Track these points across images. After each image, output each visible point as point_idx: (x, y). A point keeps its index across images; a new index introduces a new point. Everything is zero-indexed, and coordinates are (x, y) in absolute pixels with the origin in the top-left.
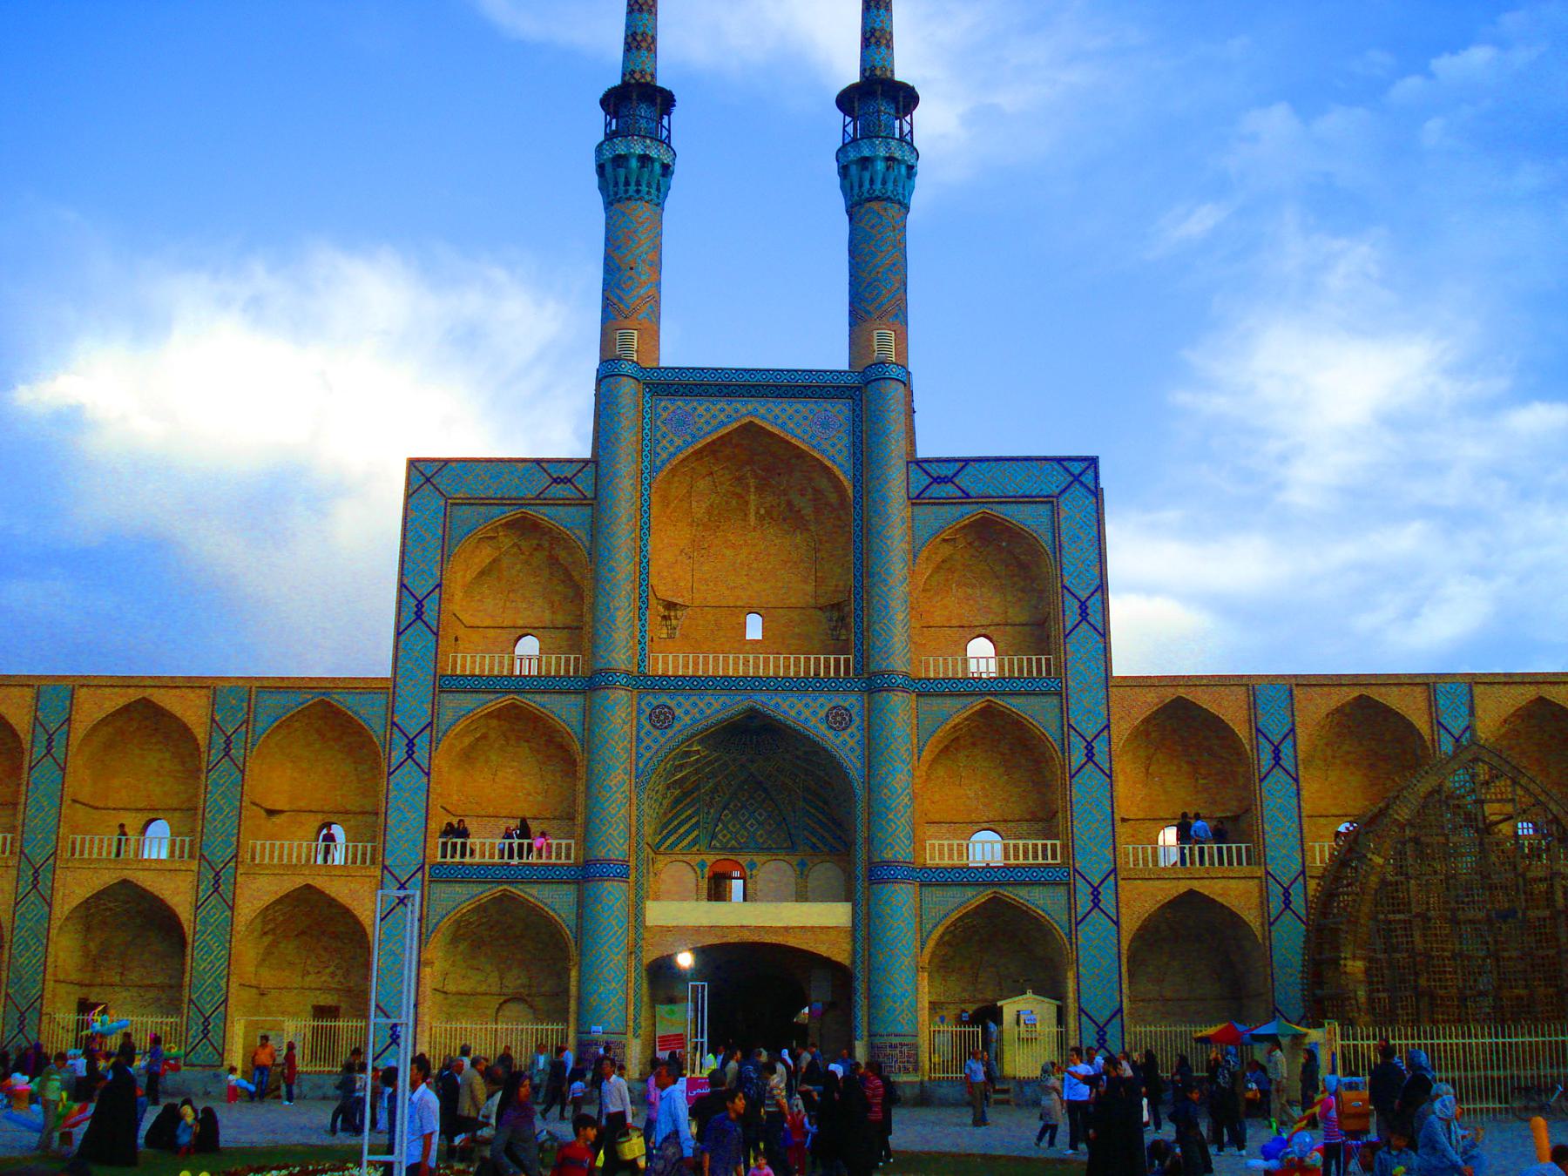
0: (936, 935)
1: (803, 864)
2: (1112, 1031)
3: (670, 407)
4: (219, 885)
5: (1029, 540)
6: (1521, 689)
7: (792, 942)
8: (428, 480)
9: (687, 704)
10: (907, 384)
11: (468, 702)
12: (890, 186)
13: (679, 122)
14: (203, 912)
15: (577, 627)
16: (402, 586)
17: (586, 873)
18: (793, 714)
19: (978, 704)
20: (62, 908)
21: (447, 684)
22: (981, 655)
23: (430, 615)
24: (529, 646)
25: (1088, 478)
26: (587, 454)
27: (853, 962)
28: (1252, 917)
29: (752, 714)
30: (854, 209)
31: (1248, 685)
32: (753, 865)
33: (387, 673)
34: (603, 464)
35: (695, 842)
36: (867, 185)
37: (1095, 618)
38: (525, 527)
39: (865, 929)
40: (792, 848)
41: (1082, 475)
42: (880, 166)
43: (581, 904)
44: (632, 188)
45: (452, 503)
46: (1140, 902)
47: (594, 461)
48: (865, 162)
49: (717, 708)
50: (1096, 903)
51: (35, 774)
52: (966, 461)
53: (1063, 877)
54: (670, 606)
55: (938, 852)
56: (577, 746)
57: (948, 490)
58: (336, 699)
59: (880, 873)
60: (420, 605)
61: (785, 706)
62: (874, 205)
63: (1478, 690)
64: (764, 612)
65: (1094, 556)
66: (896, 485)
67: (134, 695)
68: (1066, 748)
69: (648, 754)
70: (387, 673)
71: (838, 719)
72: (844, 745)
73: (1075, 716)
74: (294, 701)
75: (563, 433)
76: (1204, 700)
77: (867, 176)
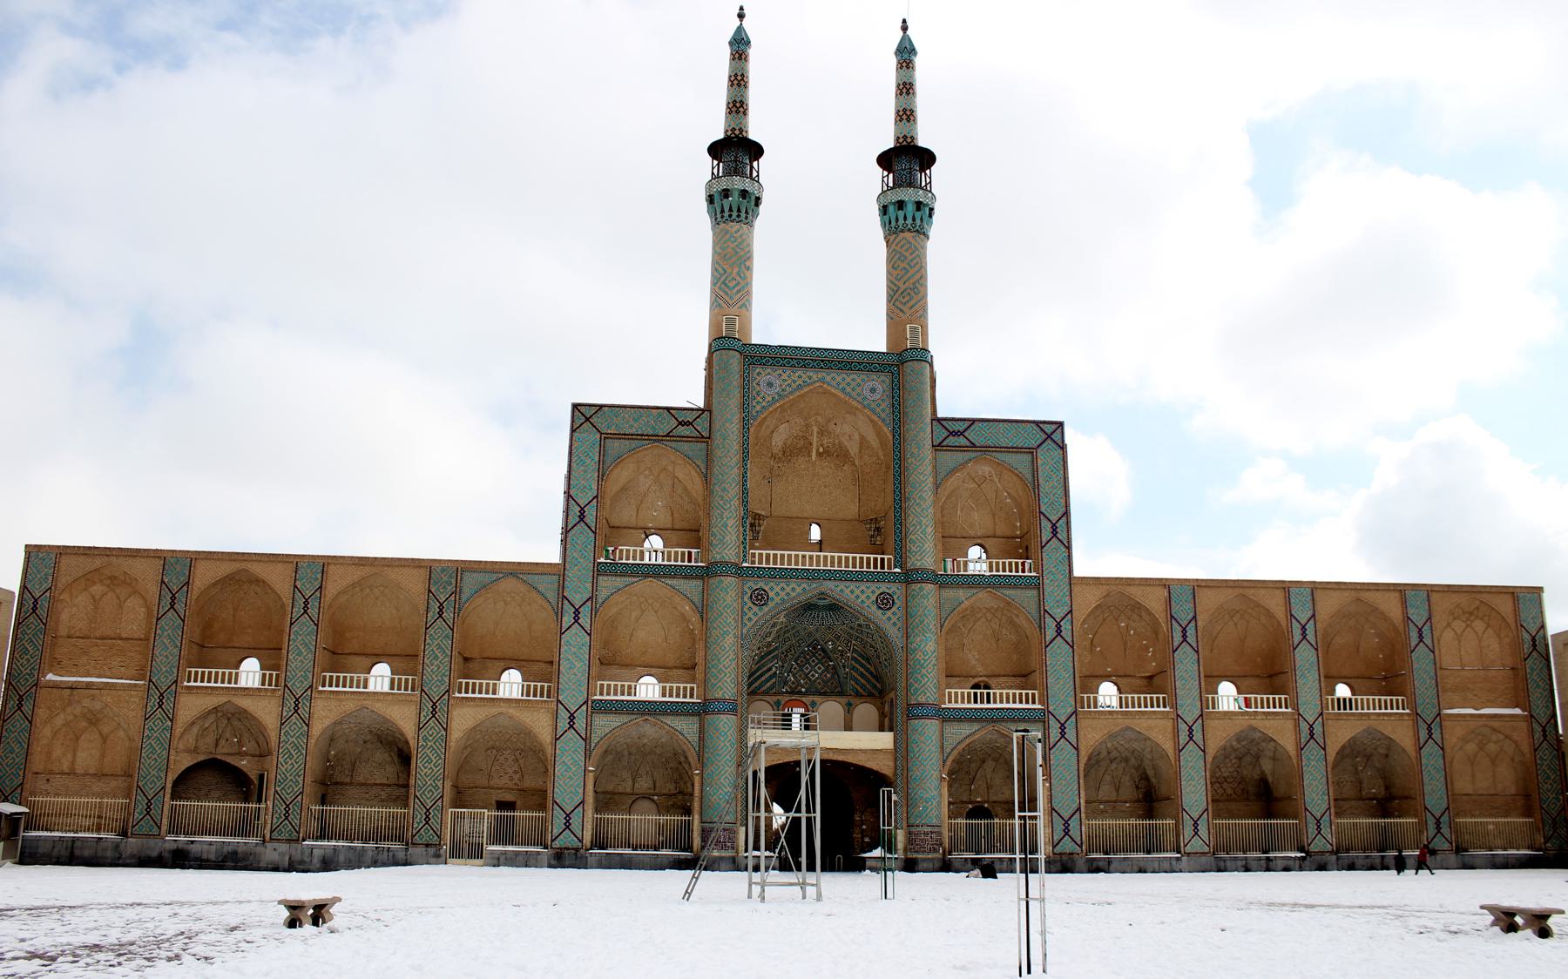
0: (951, 758)
1: (850, 704)
2: (1073, 823)
4: (435, 710)
6: (1346, 594)
7: (850, 759)
8: (587, 419)
9: (777, 589)
10: (931, 365)
11: (619, 582)
12: (918, 222)
13: (764, 165)
14: (424, 733)
16: (568, 496)
18: (853, 597)
20: (317, 729)
23: (590, 519)
24: (656, 542)
25: (1056, 436)
26: (702, 405)
27: (895, 774)
28: (1168, 746)
29: (822, 596)
31: (1165, 584)
32: (814, 704)
34: (715, 412)
35: (773, 686)
36: (901, 221)
37: (1062, 535)
40: (841, 694)
41: (1052, 433)
42: (910, 208)
43: (702, 731)
44: (735, 214)
45: (605, 437)
47: (708, 409)
48: (901, 205)
49: (798, 591)
50: (1063, 734)
51: (295, 628)
54: (757, 517)
59: (914, 711)
60: (582, 511)
61: (847, 591)
62: (907, 235)
63: (1318, 594)
65: (1061, 492)
66: (922, 439)
68: (1042, 628)
69: (749, 624)
71: (885, 602)
72: (889, 623)
73: (1049, 605)
77: (901, 214)
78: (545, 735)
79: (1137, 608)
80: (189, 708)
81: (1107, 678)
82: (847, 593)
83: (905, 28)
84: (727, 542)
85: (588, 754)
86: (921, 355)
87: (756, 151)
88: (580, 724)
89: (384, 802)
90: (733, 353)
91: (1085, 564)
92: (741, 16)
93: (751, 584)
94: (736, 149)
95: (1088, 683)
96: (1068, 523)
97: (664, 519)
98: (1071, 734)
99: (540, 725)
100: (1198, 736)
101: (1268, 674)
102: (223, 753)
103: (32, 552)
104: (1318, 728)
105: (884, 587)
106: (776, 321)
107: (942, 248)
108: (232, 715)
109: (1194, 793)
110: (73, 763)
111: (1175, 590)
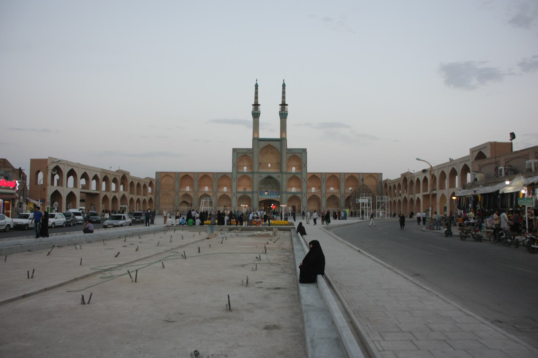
5: (299, 156)
21: (238, 173)
22: (294, 169)
24: (245, 168)
30: (281, 118)
33: (231, 171)
38: (245, 155)
39: (281, 198)
45: (238, 153)
46: (309, 196)
49: (266, 175)
52: (292, 149)
55: (289, 190)
59: (282, 193)
64: (271, 164)
66: (284, 153)
70: (231, 171)
71: (279, 177)
72: (279, 180)
75: (250, 146)
76: (316, 175)
79: (317, 177)
80: (181, 194)
84: (256, 170)
86: (285, 139)
90: (256, 140)
91: (309, 171)
93: (259, 175)
95: (309, 188)
102: (186, 200)
103: (157, 173)
107: (289, 120)
108: (187, 195)
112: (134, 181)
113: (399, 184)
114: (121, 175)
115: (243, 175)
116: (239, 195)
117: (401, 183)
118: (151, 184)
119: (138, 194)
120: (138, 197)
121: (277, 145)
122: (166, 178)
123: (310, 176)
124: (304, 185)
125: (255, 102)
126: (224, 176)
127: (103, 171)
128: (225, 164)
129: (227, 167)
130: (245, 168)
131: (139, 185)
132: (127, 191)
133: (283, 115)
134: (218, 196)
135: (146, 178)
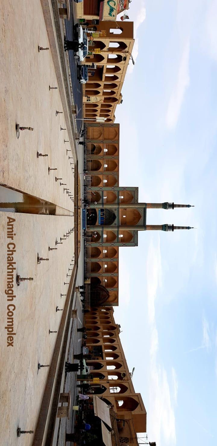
3: (143, 210)
4: (102, 173)
15: (124, 202)
17: (103, 204)
19: (117, 235)
21: (118, 192)
26: (139, 202)
28: (99, 257)
30: (162, 226)
31: (118, 257)
33: (120, 186)
37: (124, 245)
38: (132, 197)
39: (98, 226)
41: (136, 245)
45: (134, 192)
46: (100, 248)
48: (166, 227)
49: (116, 214)
53: (102, 242)
55: (104, 232)
56: (113, 203)
57: (135, 234)
58: (117, 183)
59: (103, 228)
67: (117, 164)
71: (115, 224)
72: (113, 225)
74: (117, 179)
78: (100, 185)
80: (101, 145)
81: (107, 251)
82: (116, 220)
83: (192, 228)
85: (97, 191)
86: (145, 229)
87: (173, 209)
88: (101, 190)
89: (91, 167)
92: (193, 206)
94: (173, 206)
95: (107, 249)
96: (125, 246)
97: (125, 198)
98: (100, 246)
99: (101, 185)
100: (100, 261)
101: (107, 271)
103: (119, 124)
104: (101, 275)
105: (117, 224)
106: (150, 212)
107: (160, 233)
108: (100, 150)
109: (94, 260)
110: (95, 132)
111: (117, 259)
112: (112, 107)
113: (110, 322)
114: (117, 98)
115: (117, 195)
116: (101, 193)
117: (111, 324)
118: (109, 120)
119: (101, 111)
120: (99, 111)
121: (141, 222)
122: (115, 132)
123: (116, 249)
124: (108, 244)
125: (176, 205)
126: (116, 181)
127: (121, 84)
128: (125, 180)
129: (124, 182)
130: (122, 197)
131: (109, 111)
132: (104, 102)
133: (165, 227)
134: (99, 176)
135: (114, 116)
